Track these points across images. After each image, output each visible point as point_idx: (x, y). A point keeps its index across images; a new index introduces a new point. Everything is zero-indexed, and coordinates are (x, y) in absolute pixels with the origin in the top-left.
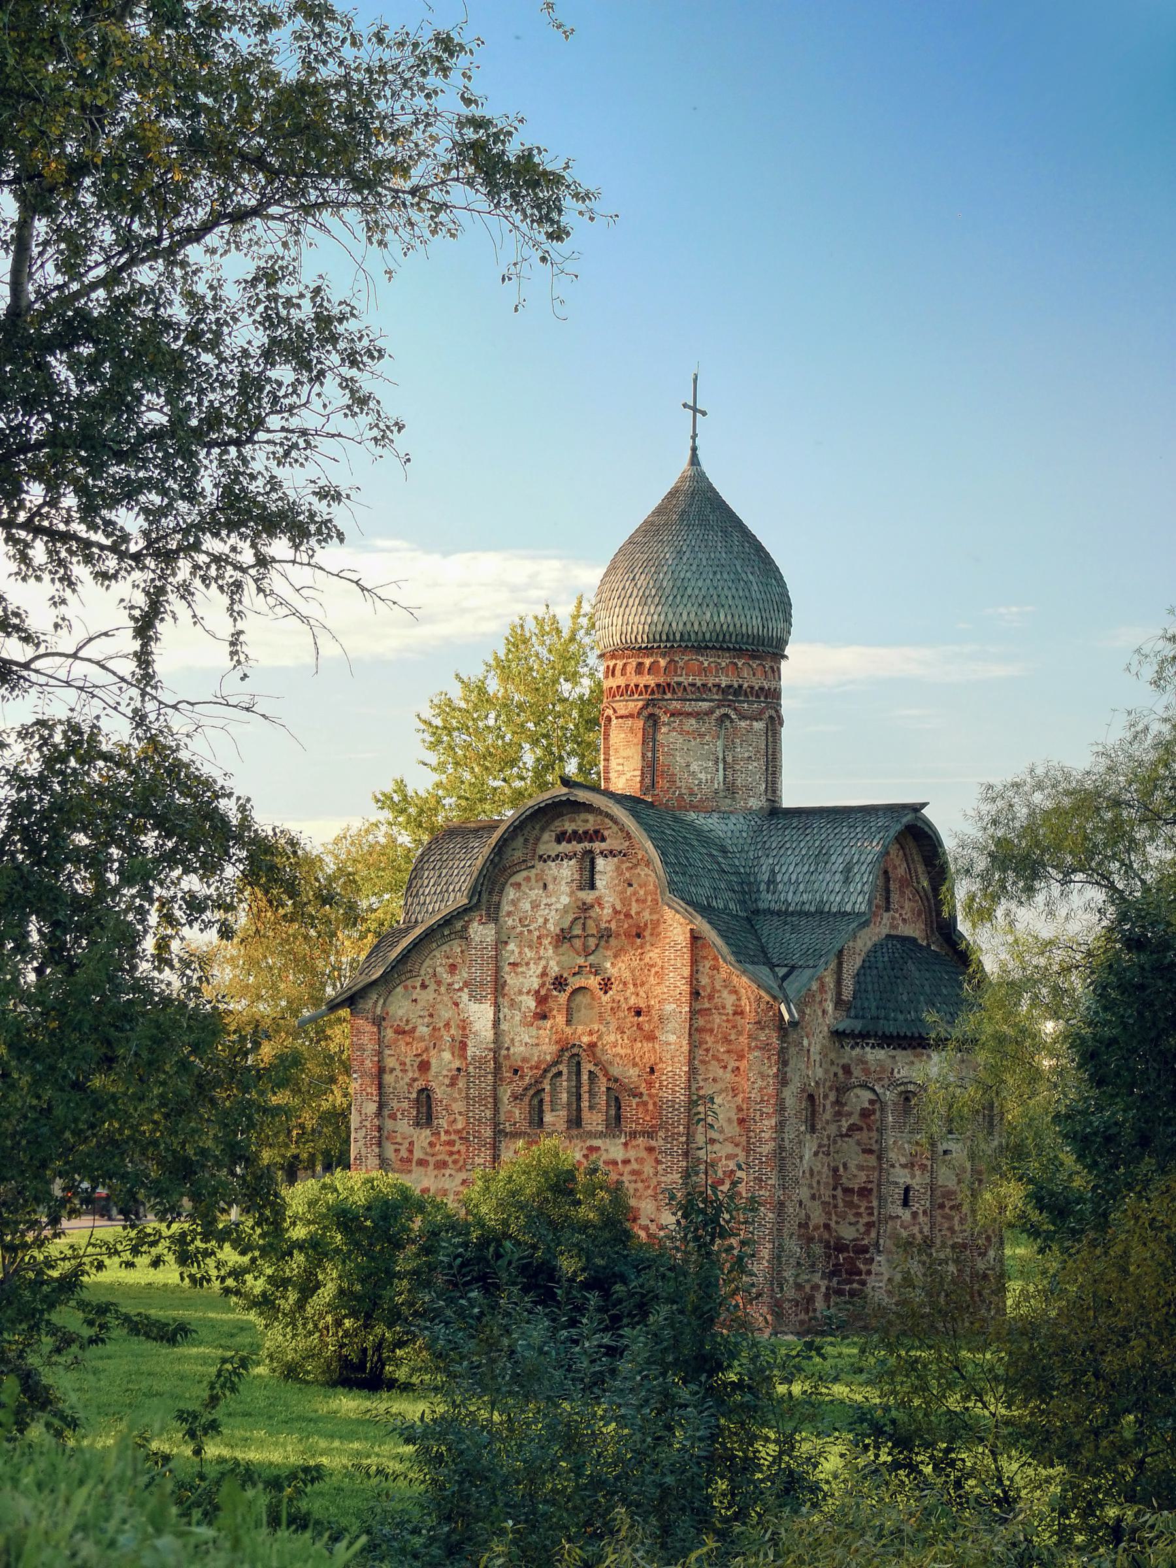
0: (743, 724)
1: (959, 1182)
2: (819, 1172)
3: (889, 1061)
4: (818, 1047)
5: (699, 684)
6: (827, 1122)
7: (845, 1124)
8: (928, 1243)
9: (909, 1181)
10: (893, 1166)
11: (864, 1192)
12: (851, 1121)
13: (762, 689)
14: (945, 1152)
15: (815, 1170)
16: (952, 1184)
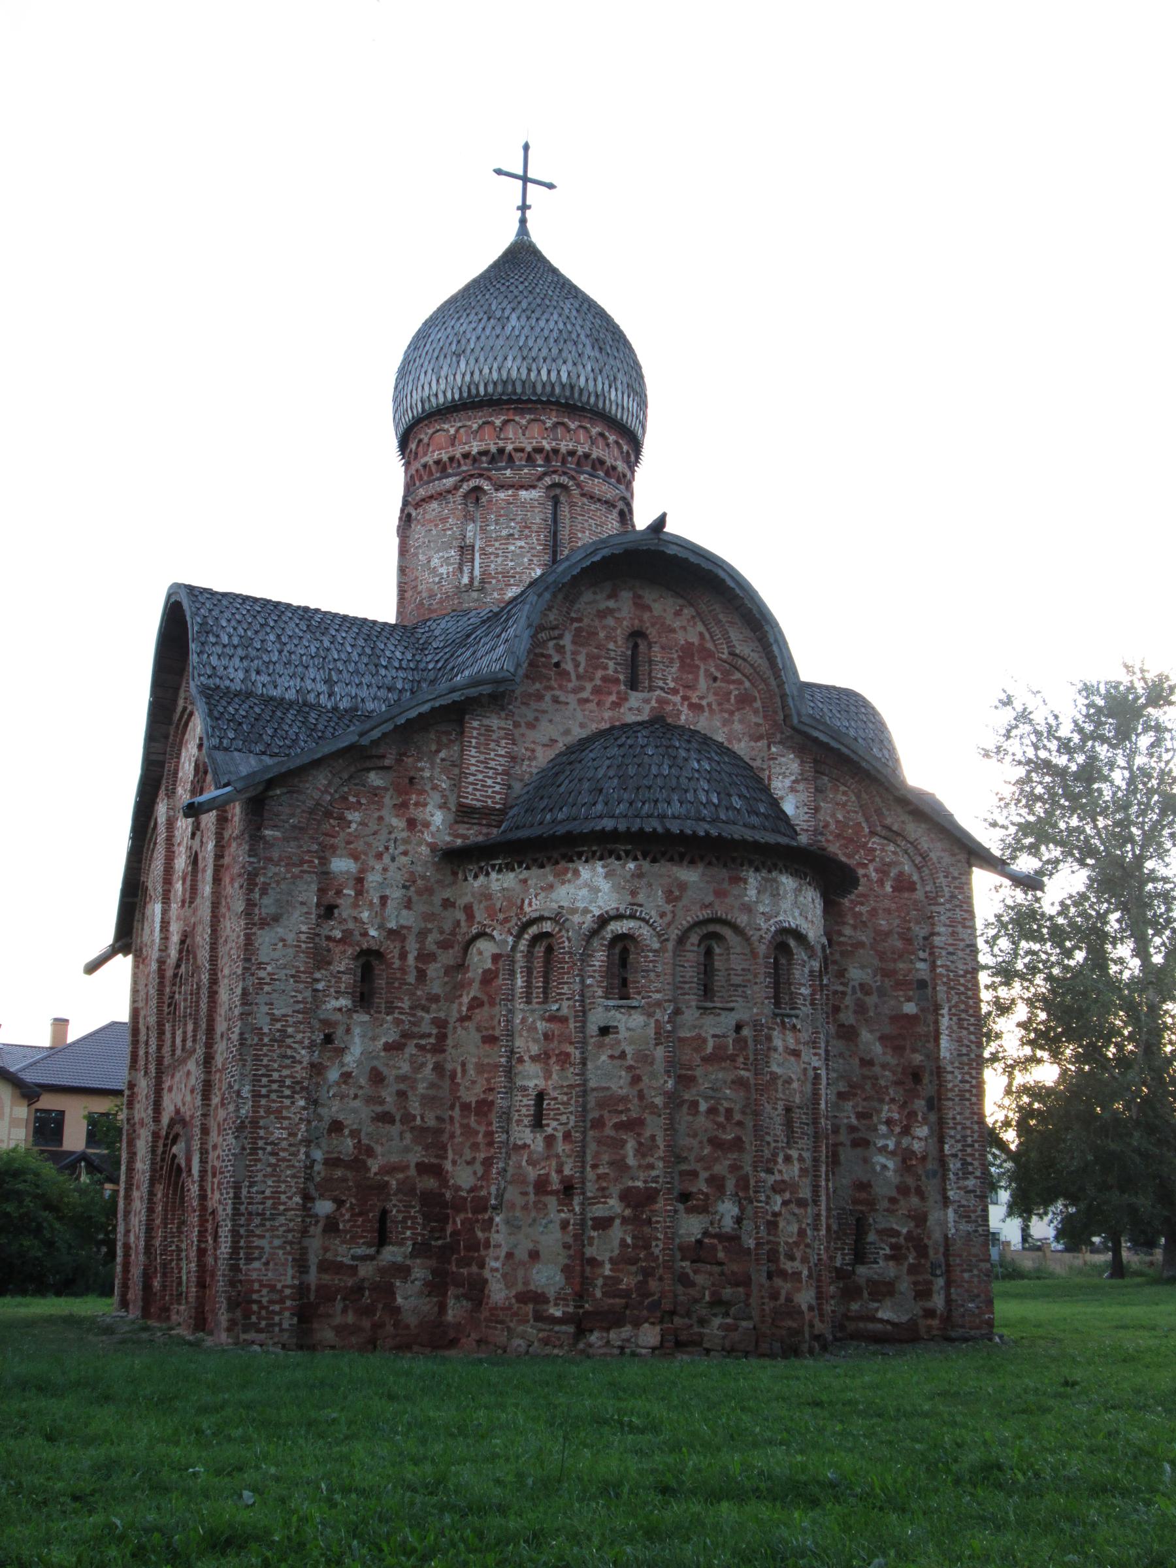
0: (501, 495)
1: (636, 1080)
2: (403, 1078)
3: (519, 888)
4: (396, 876)
5: (445, 458)
6: (435, 999)
7: (465, 1000)
8: (568, 1189)
9: (541, 1083)
10: (521, 1060)
11: (483, 1107)
12: (472, 994)
13: (539, 450)
14: (605, 1031)
15: (390, 1074)
16: (619, 1084)
